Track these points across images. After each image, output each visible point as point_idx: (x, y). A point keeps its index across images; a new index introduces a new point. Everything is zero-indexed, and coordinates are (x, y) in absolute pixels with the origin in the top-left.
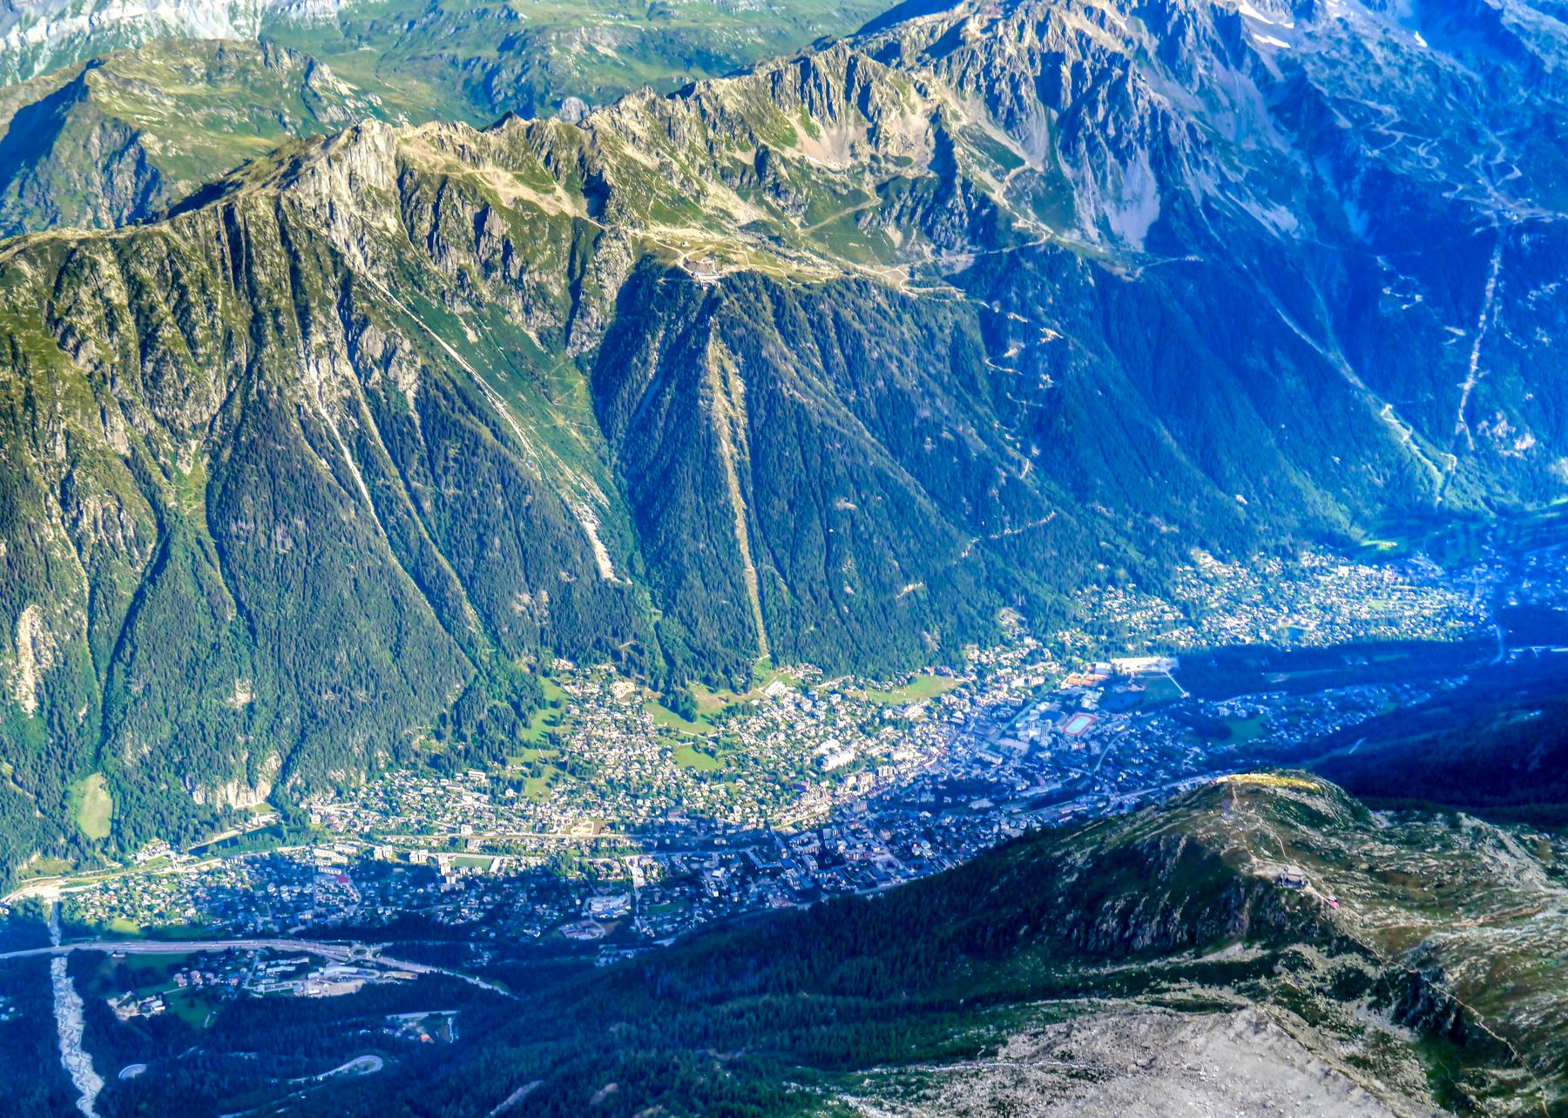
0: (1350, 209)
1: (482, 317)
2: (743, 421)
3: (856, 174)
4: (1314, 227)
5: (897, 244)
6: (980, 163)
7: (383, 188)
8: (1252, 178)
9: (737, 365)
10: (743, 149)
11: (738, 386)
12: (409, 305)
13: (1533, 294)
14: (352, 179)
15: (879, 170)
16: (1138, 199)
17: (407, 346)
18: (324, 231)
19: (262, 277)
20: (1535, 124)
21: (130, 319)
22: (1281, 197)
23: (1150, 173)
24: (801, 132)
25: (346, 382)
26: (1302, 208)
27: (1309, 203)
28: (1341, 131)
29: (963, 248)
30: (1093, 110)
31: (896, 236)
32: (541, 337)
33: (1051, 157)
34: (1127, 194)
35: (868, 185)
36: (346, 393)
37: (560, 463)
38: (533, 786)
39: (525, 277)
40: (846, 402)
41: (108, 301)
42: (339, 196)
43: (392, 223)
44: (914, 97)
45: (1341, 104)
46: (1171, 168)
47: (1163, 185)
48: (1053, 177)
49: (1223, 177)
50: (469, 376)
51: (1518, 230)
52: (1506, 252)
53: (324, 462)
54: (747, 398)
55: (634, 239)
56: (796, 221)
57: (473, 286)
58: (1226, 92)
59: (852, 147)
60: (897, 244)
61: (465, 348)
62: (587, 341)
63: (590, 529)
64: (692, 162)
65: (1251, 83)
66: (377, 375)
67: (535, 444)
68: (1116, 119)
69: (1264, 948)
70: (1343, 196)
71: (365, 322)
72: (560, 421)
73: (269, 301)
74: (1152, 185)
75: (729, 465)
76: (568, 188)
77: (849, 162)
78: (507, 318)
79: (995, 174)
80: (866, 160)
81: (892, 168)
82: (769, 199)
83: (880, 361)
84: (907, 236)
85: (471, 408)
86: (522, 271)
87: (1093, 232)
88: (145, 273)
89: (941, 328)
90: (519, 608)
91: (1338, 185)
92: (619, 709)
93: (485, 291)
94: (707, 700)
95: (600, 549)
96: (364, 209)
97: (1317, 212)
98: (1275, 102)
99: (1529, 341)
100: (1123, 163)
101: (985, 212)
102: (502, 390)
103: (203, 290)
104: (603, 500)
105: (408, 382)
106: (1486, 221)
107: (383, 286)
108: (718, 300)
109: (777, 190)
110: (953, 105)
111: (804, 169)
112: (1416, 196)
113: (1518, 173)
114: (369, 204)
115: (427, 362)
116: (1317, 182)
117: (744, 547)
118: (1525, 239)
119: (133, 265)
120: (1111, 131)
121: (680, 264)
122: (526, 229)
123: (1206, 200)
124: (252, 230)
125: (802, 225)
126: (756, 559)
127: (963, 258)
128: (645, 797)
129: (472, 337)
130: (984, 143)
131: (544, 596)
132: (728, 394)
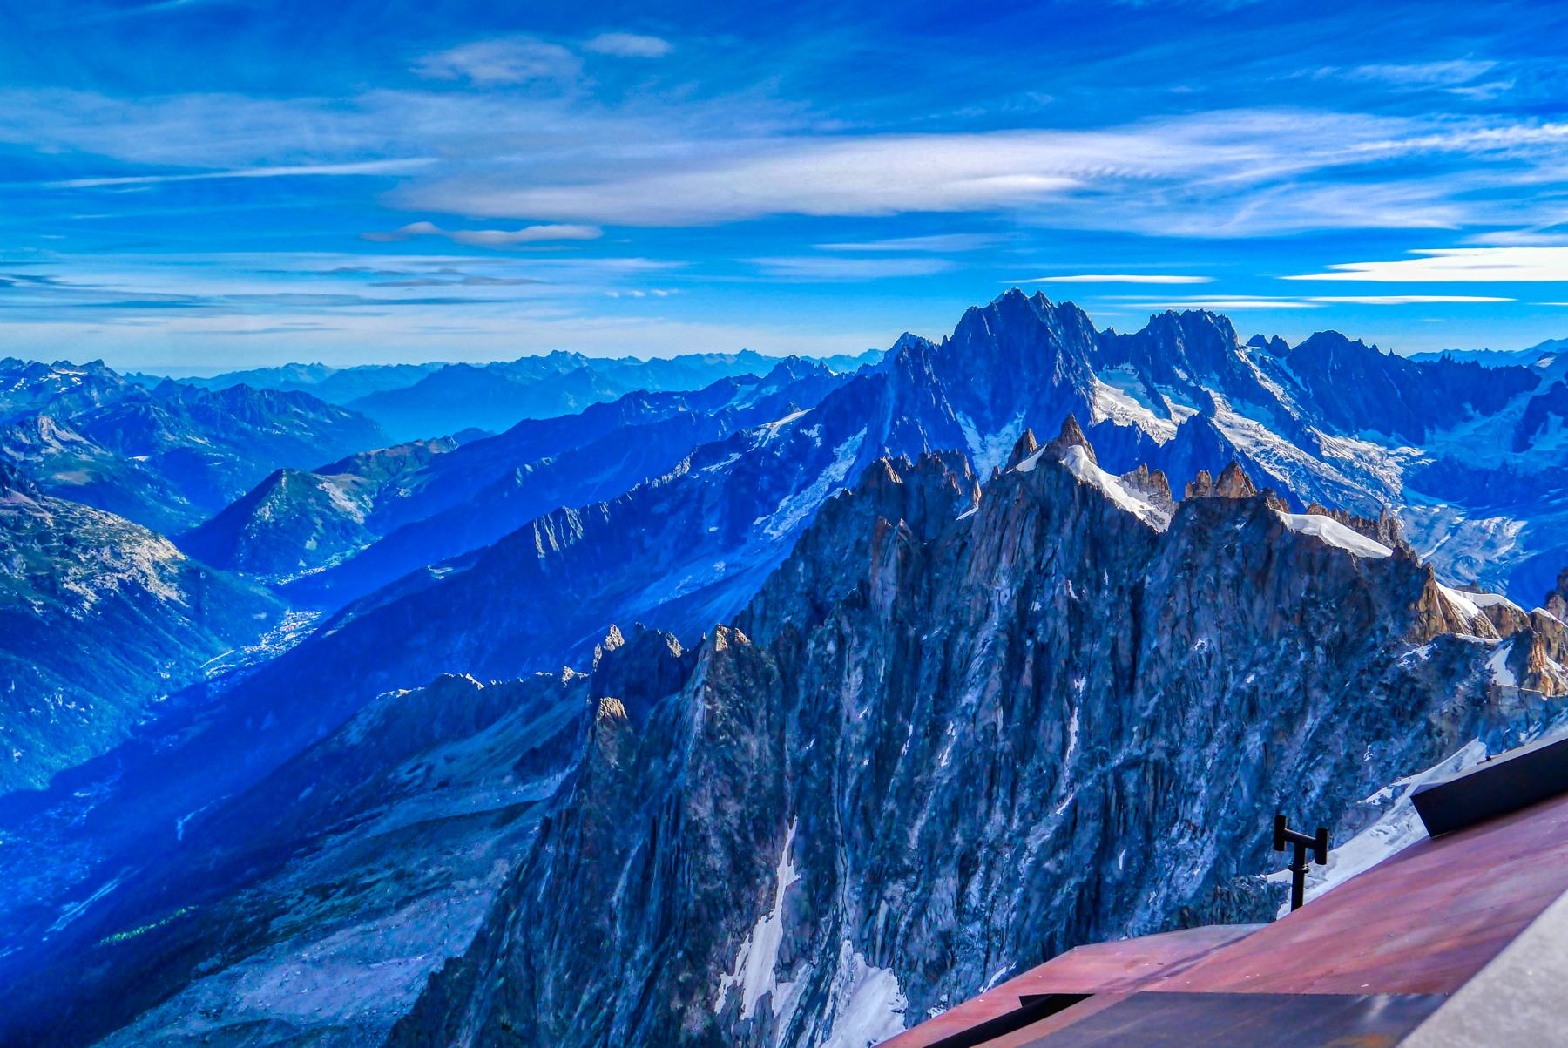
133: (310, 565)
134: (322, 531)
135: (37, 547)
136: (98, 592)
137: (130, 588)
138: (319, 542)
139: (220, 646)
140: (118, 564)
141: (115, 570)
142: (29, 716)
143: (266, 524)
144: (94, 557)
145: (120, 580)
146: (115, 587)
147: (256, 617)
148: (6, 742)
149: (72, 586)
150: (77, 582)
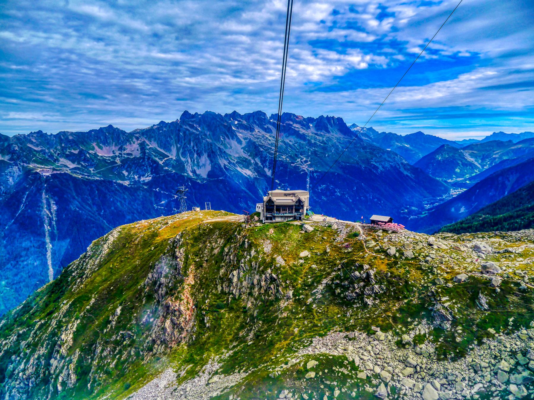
0: (266, 170)
3: (114, 158)
4: (256, 174)
5: (126, 175)
6: (155, 156)
8: (237, 162)
9: (55, 201)
10: (74, 150)
13: (320, 188)
15: (121, 157)
16: (204, 165)
20: (312, 153)
22: (247, 167)
23: (207, 158)
24: (96, 148)
26: (253, 170)
27: (255, 169)
28: (261, 151)
29: (148, 176)
30: (190, 144)
31: (126, 174)
33: (178, 155)
34: (201, 164)
35: (118, 161)
40: (99, 214)
44: (134, 140)
45: (261, 146)
46: (214, 157)
47: (212, 161)
48: (178, 160)
49: (229, 161)
51: (312, 172)
52: (310, 177)
54: (57, 211)
55: (23, 166)
56: (91, 169)
58: (229, 145)
59: (113, 151)
60: (126, 175)
64: (55, 153)
65: (236, 143)
68: (197, 145)
69: (229, 368)
70: (264, 167)
74: (208, 162)
75: (47, 234)
77: (112, 155)
79: (160, 159)
80: (117, 154)
81: (126, 156)
82: (82, 163)
83: (113, 201)
84: (129, 174)
87: (191, 174)
89: (138, 196)
91: (262, 164)
97: (257, 170)
98: (243, 146)
99: (321, 199)
100: (200, 156)
101: (155, 165)
106: (305, 170)
108: (50, 180)
109: (85, 160)
110: (147, 142)
111: (96, 155)
112: (285, 165)
113: (309, 163)
116: (256, 164)
118: (315, 174)
120: (195, 148)
121: (38, 171)
123: (225, 166)
125: (93, 170)
127: (148, 178)
130: (156, 151)
132: (50, 210)
133: (457, 177)
134: (462, 166)
135: (362, 150)
136: (383, 167)
137: (395, 168)
138: (461, 170)
139: (428, 195)
140: (390, 159)
141: (389, 161)
142: (360, 199)
143: (440, 161)
144: (381, 156)
145: (391, 166)
146: (389, 166)
147: (440, 188)
148: (353, 206)
149: (374, 163)
150: (376, 162)
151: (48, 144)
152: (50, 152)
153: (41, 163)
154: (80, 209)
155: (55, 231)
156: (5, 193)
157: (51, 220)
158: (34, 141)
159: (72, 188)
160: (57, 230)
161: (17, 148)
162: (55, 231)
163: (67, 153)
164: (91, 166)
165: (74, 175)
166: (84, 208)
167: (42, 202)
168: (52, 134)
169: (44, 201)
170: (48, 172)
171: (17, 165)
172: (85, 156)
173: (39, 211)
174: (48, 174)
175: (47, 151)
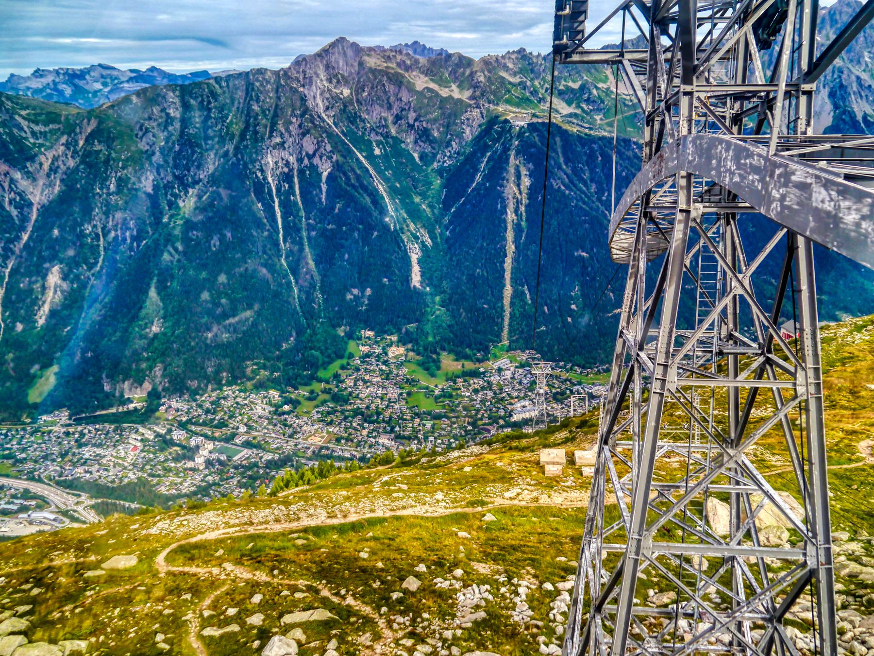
1: (387, 143)
2: (525, 201)
7: (346, 74)
9: (529, 170)
10: (574, 81)
11: (526, 182)
12: (342, 132)
14: (327, 67)
17: (329, 148)
18: (301, 89)
19: (255, 107)
21: (177, 125)
23: (827, 100)
25: (287, 164)
32: (421, 158)
36: (286, 170)
37: (409, 221)
38: (306, 406)
39: (417, 124)
41: (168, 114)
42: (318, 75)
43: (346, 92)
46: (843, 98)
47: (836, 107)
50: (367, 170)
53: (260, 205)
55: (488, 110)
56: (598, 118)
57: (386, 126)
61: (370, 157)
62: (446, 159)
63: (414, 258)
64: (542, 87)
66: (306, 161)
67: (396, 209)
71: (308, 132)
72: (417, 199)
73: (256, 119)
74: (829, 106)
75: (510, 227)
76: (458, 86)
78: (403, 145)
85: (362, 186)
86: (416, 120)
88: (193, 102)
90: (349, 297)
92: (385, 363)
93: (393, 131)
94: (449, 363)
95: (416, 269)
96: (331, 82)
102: (386, 180)
103: (221, 111)
104: (429, 242)
105: (325, 169)
107: (330, 121)
114: (334, 81)
115: (341, 159)
117: (508, 276)
119: (187, 97)
122: (426, 101)
123: (865, 118)
124: (257, 84)
126: (515, 281)
128: (373, 422)
129: (377, 152)
131: (368, 291)
132: (519, 185)
151: (532, 71)
152: (533, 85)
153: (517, 105)
154: (567, 187)
155: (523, 224)
156: (458, 154)
157: (518, 202)
158: (511, 65)
159: (559, 150)
160: (527, 220)
161: (482, 79)
162: (523, 224)
163: (561, 87)
164: (599, 110)
165: (566, 127)
166: (575, 186)
167: (507, 172)
168: (539, 55)
169: (512, 170)
170: (523, 119)
171: (478, 107)
172: (590, 93)
173: (502, 186)
174: (522, 123)
175: (529, 83)
